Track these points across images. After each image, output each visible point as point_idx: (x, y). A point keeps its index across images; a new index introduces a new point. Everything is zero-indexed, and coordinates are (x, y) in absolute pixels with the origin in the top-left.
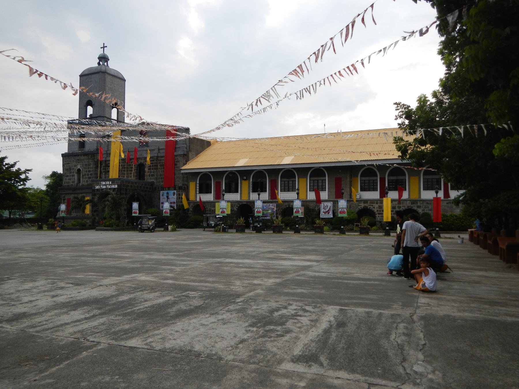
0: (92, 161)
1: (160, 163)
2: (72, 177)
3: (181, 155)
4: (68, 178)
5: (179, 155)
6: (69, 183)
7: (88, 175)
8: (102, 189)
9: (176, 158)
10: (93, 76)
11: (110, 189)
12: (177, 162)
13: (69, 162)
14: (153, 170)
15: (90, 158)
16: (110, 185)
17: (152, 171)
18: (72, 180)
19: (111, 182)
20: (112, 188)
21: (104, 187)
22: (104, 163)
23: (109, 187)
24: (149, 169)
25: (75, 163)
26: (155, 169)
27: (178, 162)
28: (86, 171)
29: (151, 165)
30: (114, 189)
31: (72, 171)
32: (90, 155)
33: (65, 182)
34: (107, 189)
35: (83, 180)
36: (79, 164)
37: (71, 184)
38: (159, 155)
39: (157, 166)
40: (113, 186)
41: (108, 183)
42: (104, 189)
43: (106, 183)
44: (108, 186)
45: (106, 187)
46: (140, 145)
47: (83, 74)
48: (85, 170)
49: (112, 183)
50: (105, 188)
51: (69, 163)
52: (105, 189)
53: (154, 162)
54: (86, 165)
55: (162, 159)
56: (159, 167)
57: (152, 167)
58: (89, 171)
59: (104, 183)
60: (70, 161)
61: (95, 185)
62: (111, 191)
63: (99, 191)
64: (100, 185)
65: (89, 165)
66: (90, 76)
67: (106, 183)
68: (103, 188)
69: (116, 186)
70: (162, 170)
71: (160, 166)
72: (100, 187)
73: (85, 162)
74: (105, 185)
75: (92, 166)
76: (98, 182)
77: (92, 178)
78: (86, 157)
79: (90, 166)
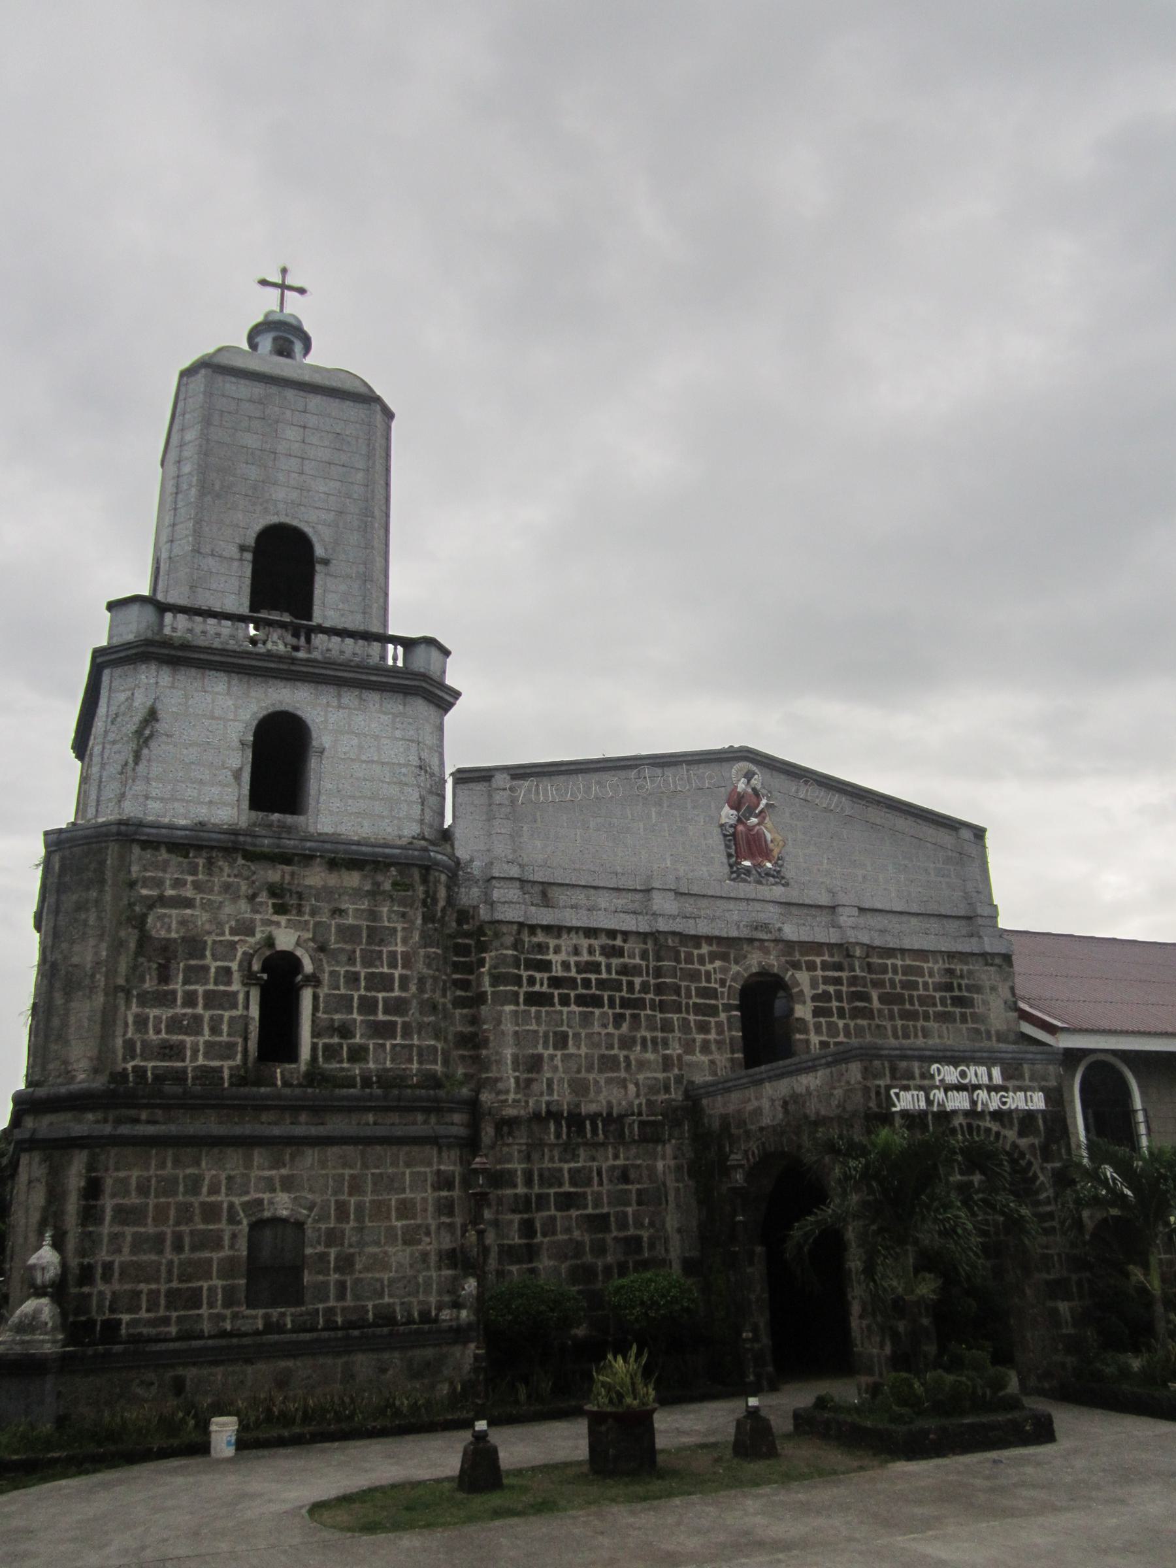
0: (404, 915)
1: (877, 984)
2: (207, 1006)
3: (993, 955)
4: (166, 1013)
5: (984, 956)
6: (172, 1051)
7: (368, 1006)
8: (944, 1116)
9: (965, 968)
10: (315, 402)
11: (998, 1115)
12: (969, 988)
13: (189, 892)
14: (841, 1015)
15: (387, 886)
16: (992, 1088)
17: (841, 1023)
18: (207, 1035)
19: (996, 1072)
20: (1010, 1111)
21: (958, 1102)
22: (509, 940)
23: (994, 1104)
24: (817, 1012)
25: (243, 905)
26: (856, 1013)
27: (978, 989)
28: (353, 979)
29: (831, 989)
30: (1027, 1119)
31: (214, 966)
32: (393, 871)
33: (129, 1045)
34: (981, 1115)
35: (321, 1042)
36: (282, 919)
37: (201, 1061)
38: (877, 943)
39: (866, 997)
40: (1017, 1101)
41: (977, 1073)
42: (954, 1112)
43: (963, 1074)
44: (982, 1095)
45: (974, 1103)
46: (748, 871)
47: (224, 360)
48: (342, 970)
49: (1006, 1076)
50: (966, 1105)
51: (188, 903)
52: (966, 1114)
53: (844, 975)
54: (349, 934)
55: (889, 962)
56: (876, 1004)
57: (835, 1004)
58: (385, 982)
59: (950, 1074)
60: (197, 886)
61: (881, 1083)
62: (1011, 1134)
63: (925, 1127)
64: (927, 1090)
65: (377, 935)
66: (290, 394)
67: (963, 1074)
68: (950, 1106)
69: (1038, 1102)
70: (899, 1023)
71: (882, 999)
72: (929, 1102)
73: (338, 912)
74: (959, 1088)
75: (400, 949)
76: (903, 1064)
77: (407, 1033)
78: (353, 879)
79: (381, 942)
